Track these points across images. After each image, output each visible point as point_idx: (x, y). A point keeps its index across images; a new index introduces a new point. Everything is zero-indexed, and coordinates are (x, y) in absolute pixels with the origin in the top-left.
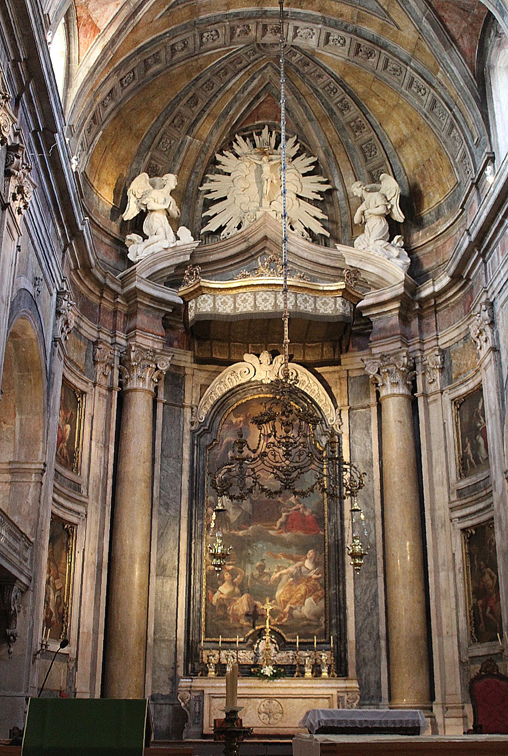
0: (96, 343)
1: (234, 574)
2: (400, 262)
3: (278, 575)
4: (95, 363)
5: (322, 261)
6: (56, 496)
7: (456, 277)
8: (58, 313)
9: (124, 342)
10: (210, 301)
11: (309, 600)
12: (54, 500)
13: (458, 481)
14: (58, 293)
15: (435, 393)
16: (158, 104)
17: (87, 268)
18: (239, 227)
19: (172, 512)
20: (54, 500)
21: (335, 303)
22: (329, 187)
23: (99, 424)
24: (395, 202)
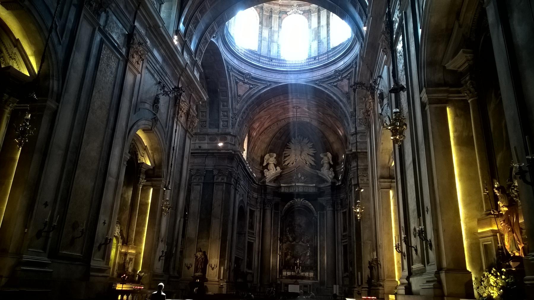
0: (257, 199)
1: (291, 253)
2: (331, 176)
3: (301, 254)
4: (257, 203)
5: (313, 173)
6: (249, 237)
7: (342, 183)
8: (248, 197)
9: (264, 197)
10: (283, 189)
11: (309, 260)
12: (248, 238)
13: (343, 233)
14: (248, 192)
15: (339, 210)
16: (271, 135)
17: (255, 182)
18: (293, 164)
19: (276, 238)
20: (248, 238)
21: (313, 189)
22: (316, 152)
23: (258, 218)
24: (331, 159)
